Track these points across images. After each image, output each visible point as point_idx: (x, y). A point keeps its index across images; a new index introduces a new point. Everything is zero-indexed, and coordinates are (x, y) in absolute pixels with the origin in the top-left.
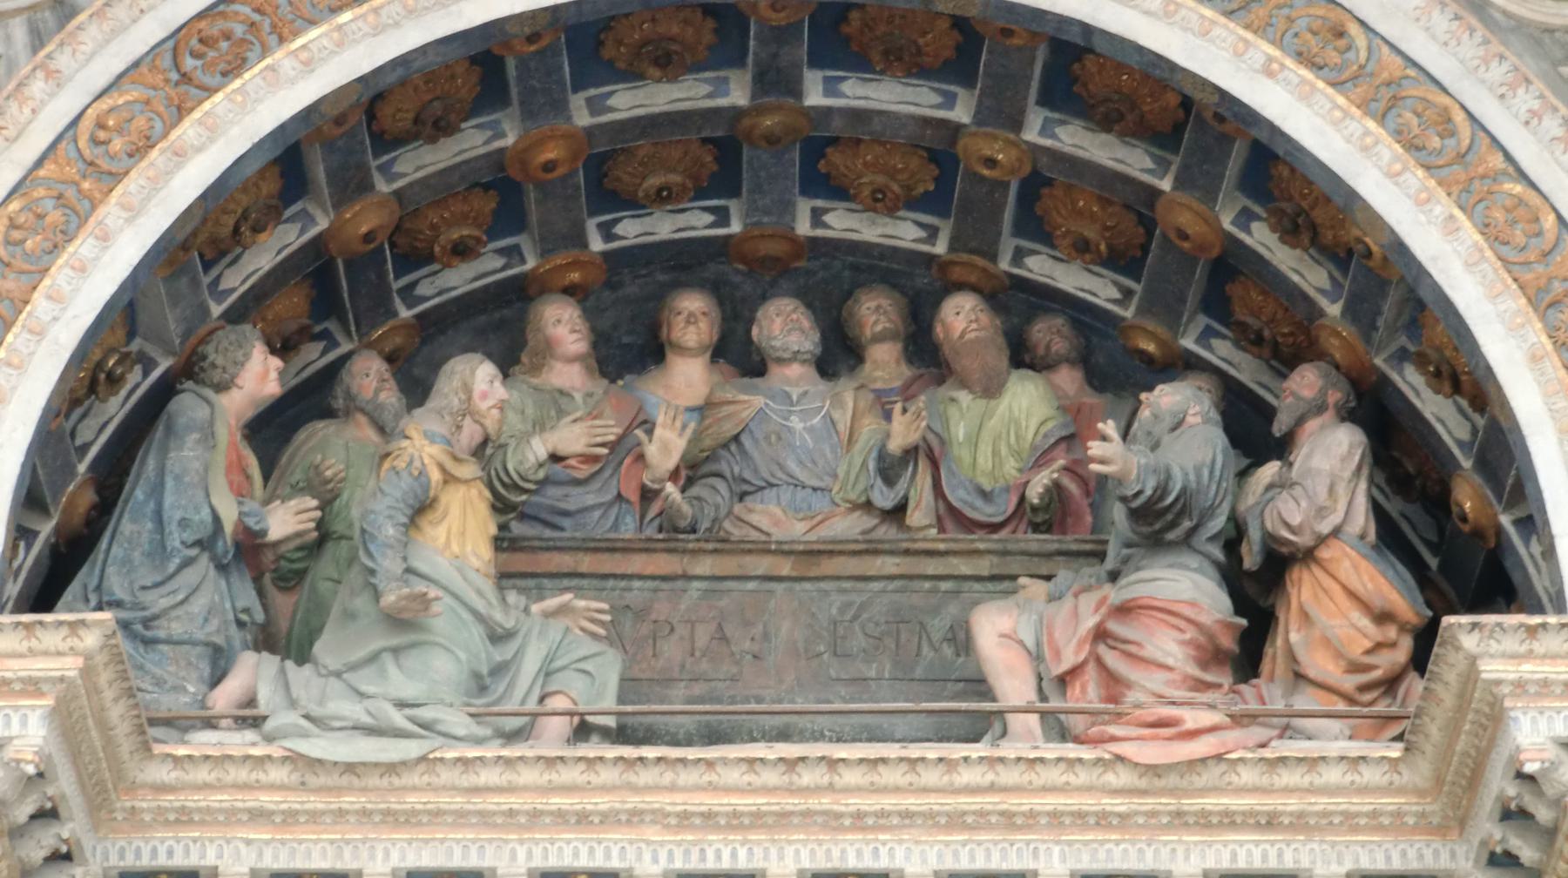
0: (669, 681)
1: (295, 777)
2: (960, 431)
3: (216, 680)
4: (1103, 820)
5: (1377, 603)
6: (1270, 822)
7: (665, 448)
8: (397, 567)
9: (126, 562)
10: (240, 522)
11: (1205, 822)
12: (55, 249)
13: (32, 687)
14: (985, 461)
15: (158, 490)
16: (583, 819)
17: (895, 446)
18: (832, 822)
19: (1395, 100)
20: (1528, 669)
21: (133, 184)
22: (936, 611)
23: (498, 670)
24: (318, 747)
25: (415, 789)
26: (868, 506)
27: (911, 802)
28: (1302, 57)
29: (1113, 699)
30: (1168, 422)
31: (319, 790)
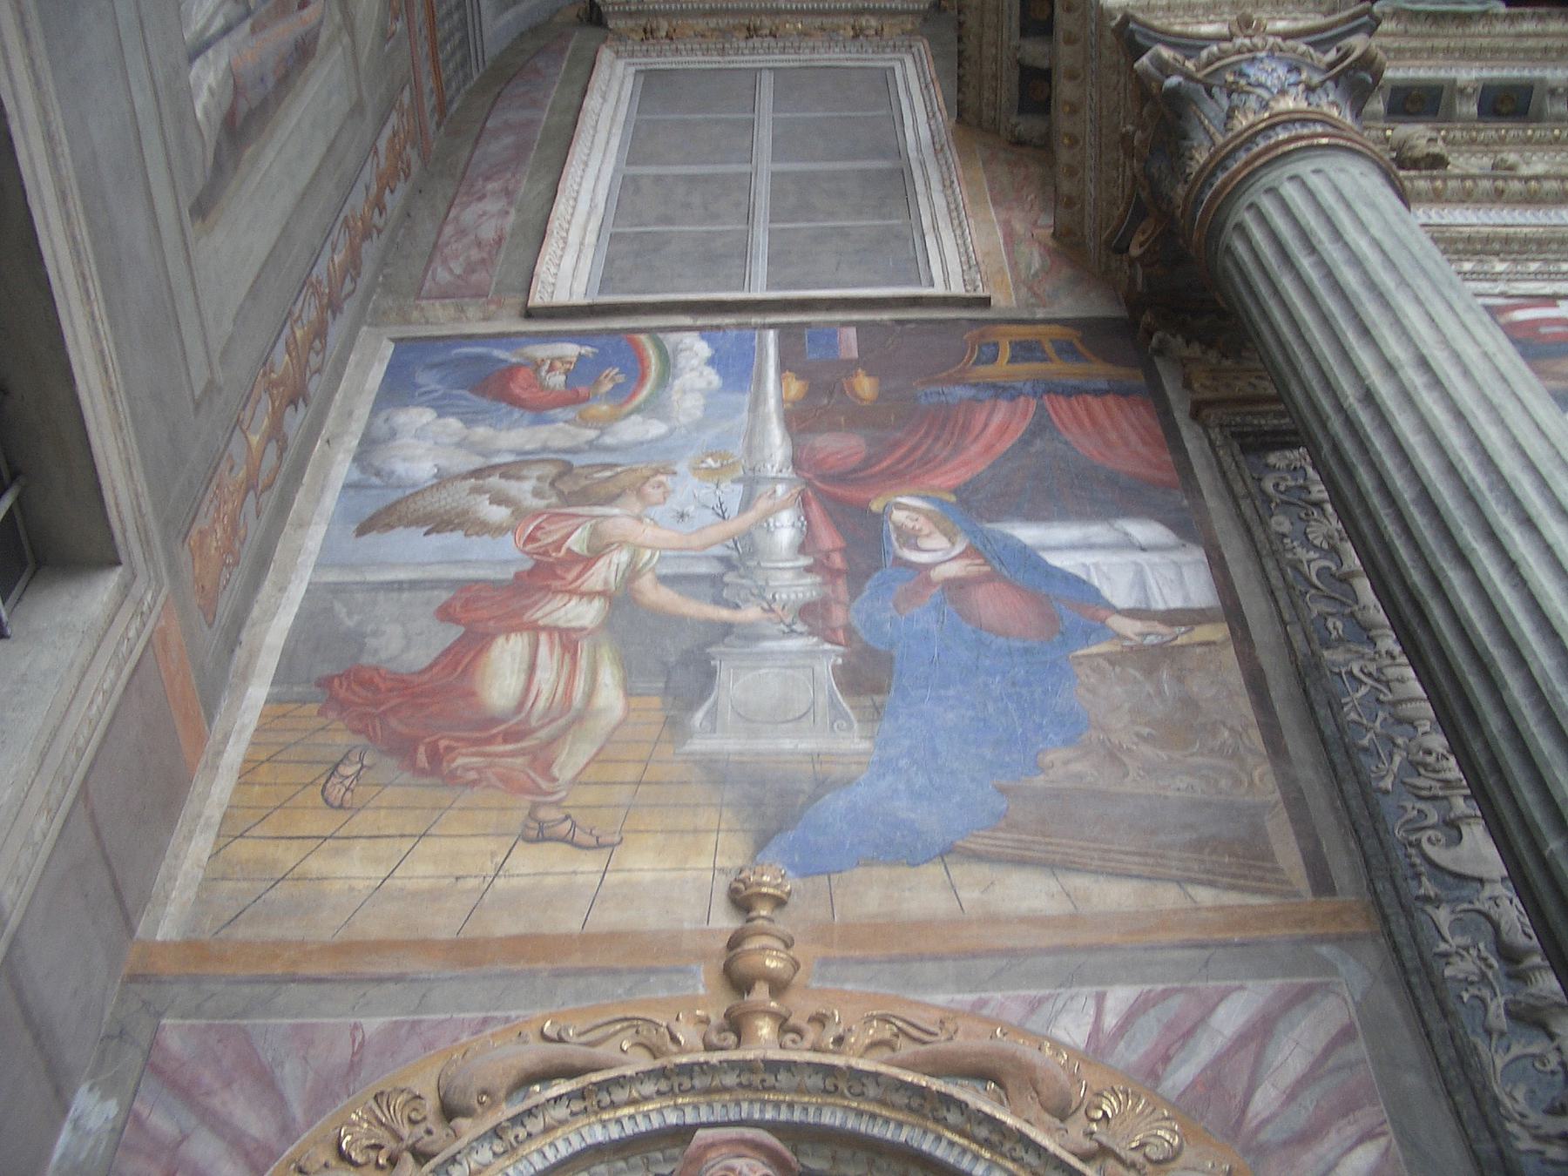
1: (1401, 27)
25: (1480, 35)
31: (1417, 36)
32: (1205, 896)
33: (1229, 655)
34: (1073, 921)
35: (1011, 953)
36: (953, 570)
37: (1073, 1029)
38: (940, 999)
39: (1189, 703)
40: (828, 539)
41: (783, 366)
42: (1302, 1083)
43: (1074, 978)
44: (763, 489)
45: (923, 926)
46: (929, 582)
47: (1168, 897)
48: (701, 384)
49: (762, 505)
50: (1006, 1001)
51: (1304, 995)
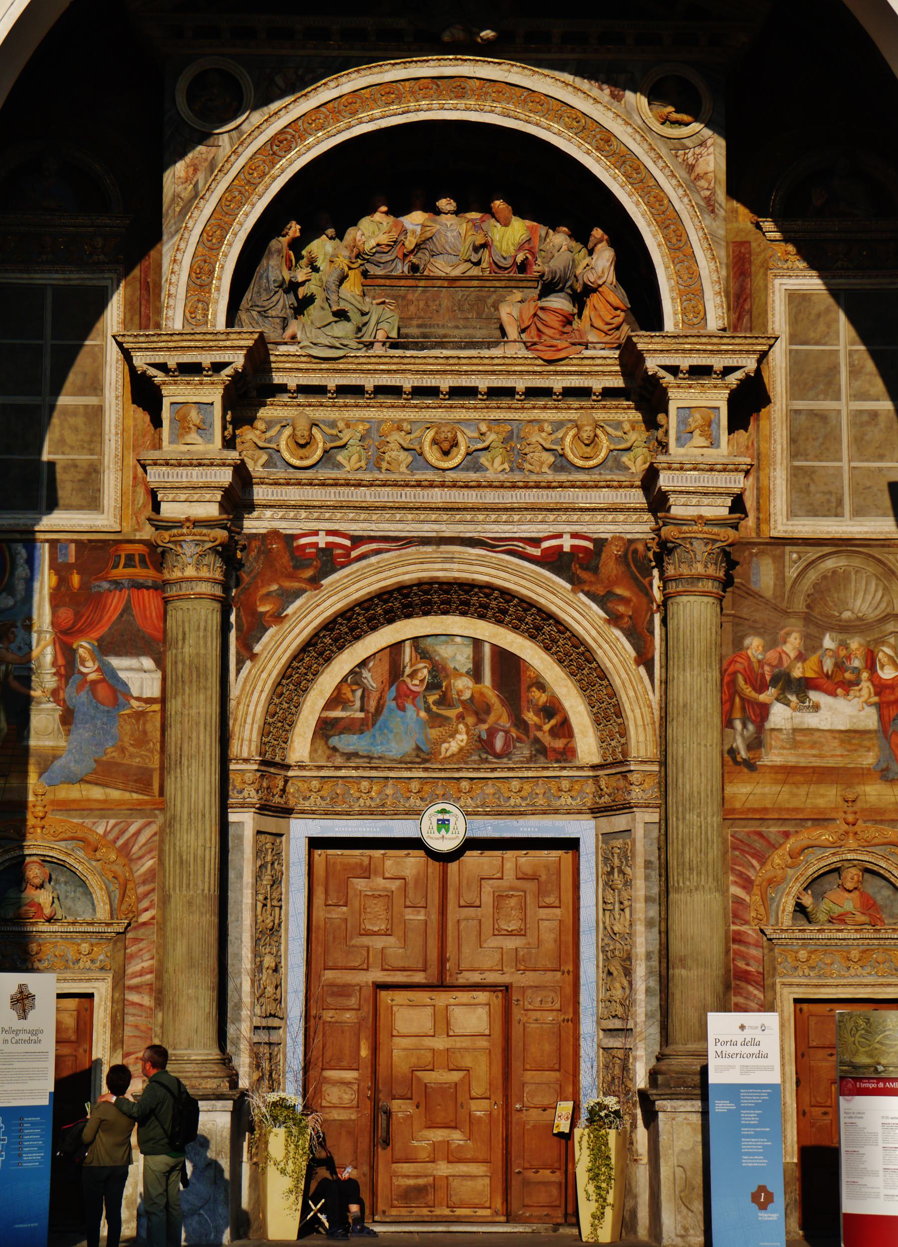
0: (411, 319)
2: (497, 237)
3: (284, 328)
4: (534, 373)
5: (615, 304)
6: (581, 373)
7: (410, 242)
8: (336, 298)
9: (259, 292)
10: (290, 281)
11: (563, 373)
12: (239, 207)
13: (241, 348)
14: (504, 247)
15: (267, 269)
16: (389, 371)
17: (477, 243)
18: (459, 373)
19: (624, 162)
20: (650, 347)
21: (260, 188)
22: (489, 297)
23: (365, 324)
24: (316, 352)
26: (470, 261)
27: (480, 368)
28: (598, 149)
29: (539, 337)
30: (557, 248)
32: (135, 796)
33: (158, 717)
34: (105, 801)
35: (91, 810)
36: (93, 677)
37: (101, 831)
38: (75, 821)
39: (145, 733)
40: (61, 661)
41: (51, 567)
42: (144, 845)
43: (102, 817)
44: (43, 636)
45: (74, 801)
46: (86, 681)
47: (127, 795)
48: (24, 575)
49: (42, 643)
50: (88, 822)
51: (149, 824)
